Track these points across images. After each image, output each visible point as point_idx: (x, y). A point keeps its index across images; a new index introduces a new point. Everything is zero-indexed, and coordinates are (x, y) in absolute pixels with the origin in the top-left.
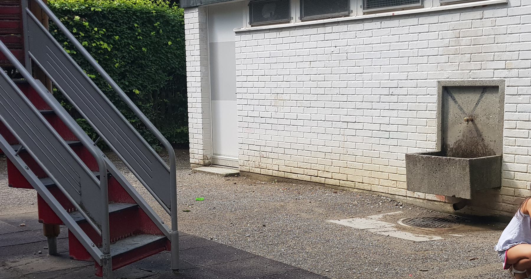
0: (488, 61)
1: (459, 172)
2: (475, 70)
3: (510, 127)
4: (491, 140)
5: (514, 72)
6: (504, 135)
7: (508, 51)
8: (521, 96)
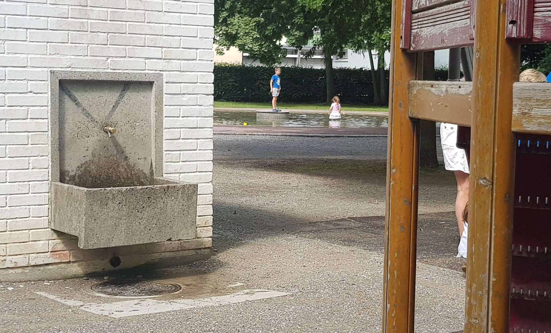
0: (136, 46)
1: (181, 204)
2: (116, 57)
3: (172, 137)
4: (140, 158)
5: (175, 64)
6: (164, 149)
7: (165, 35)
8: (186, 95)
